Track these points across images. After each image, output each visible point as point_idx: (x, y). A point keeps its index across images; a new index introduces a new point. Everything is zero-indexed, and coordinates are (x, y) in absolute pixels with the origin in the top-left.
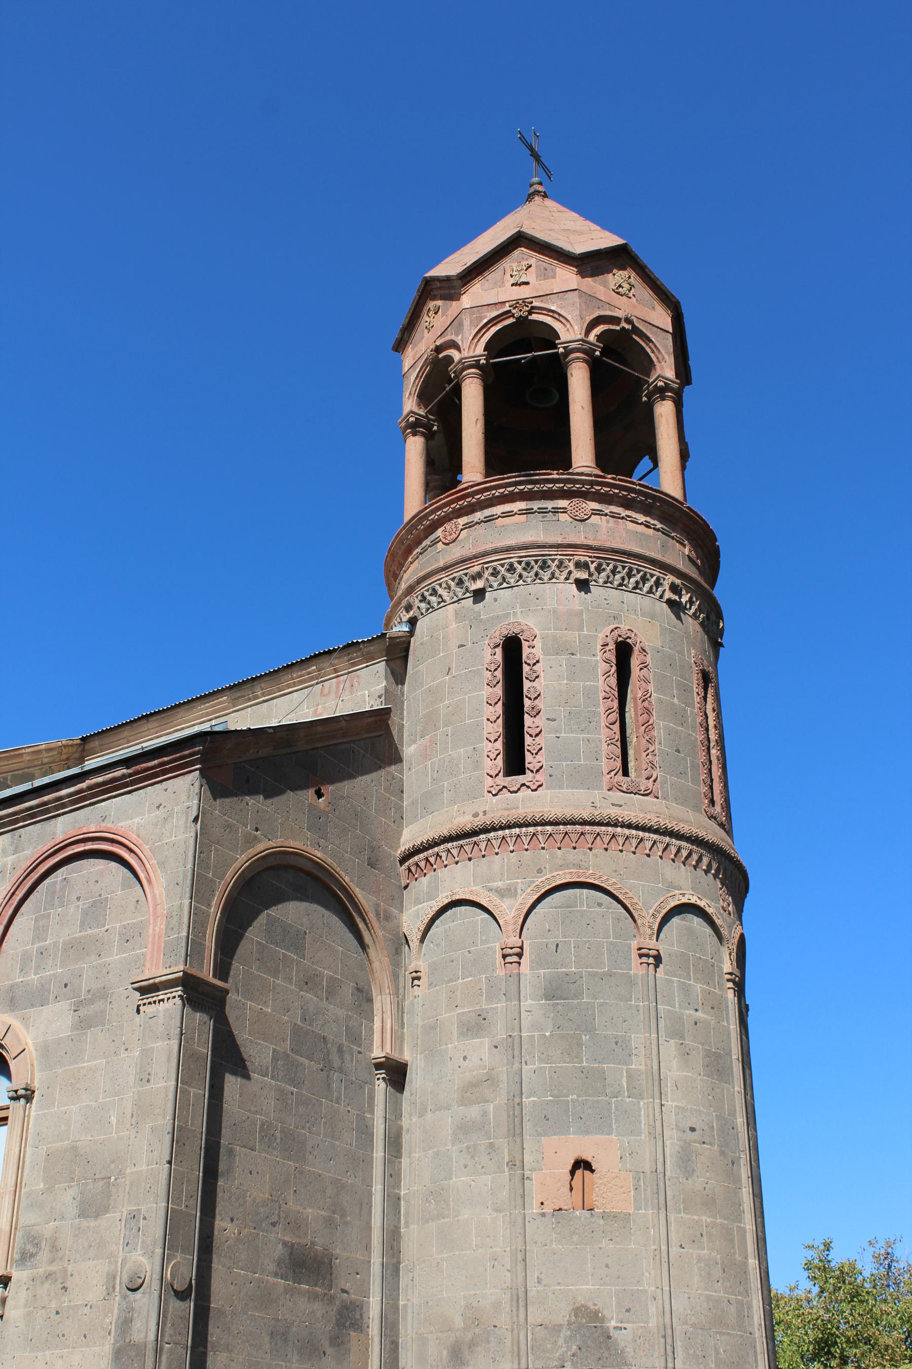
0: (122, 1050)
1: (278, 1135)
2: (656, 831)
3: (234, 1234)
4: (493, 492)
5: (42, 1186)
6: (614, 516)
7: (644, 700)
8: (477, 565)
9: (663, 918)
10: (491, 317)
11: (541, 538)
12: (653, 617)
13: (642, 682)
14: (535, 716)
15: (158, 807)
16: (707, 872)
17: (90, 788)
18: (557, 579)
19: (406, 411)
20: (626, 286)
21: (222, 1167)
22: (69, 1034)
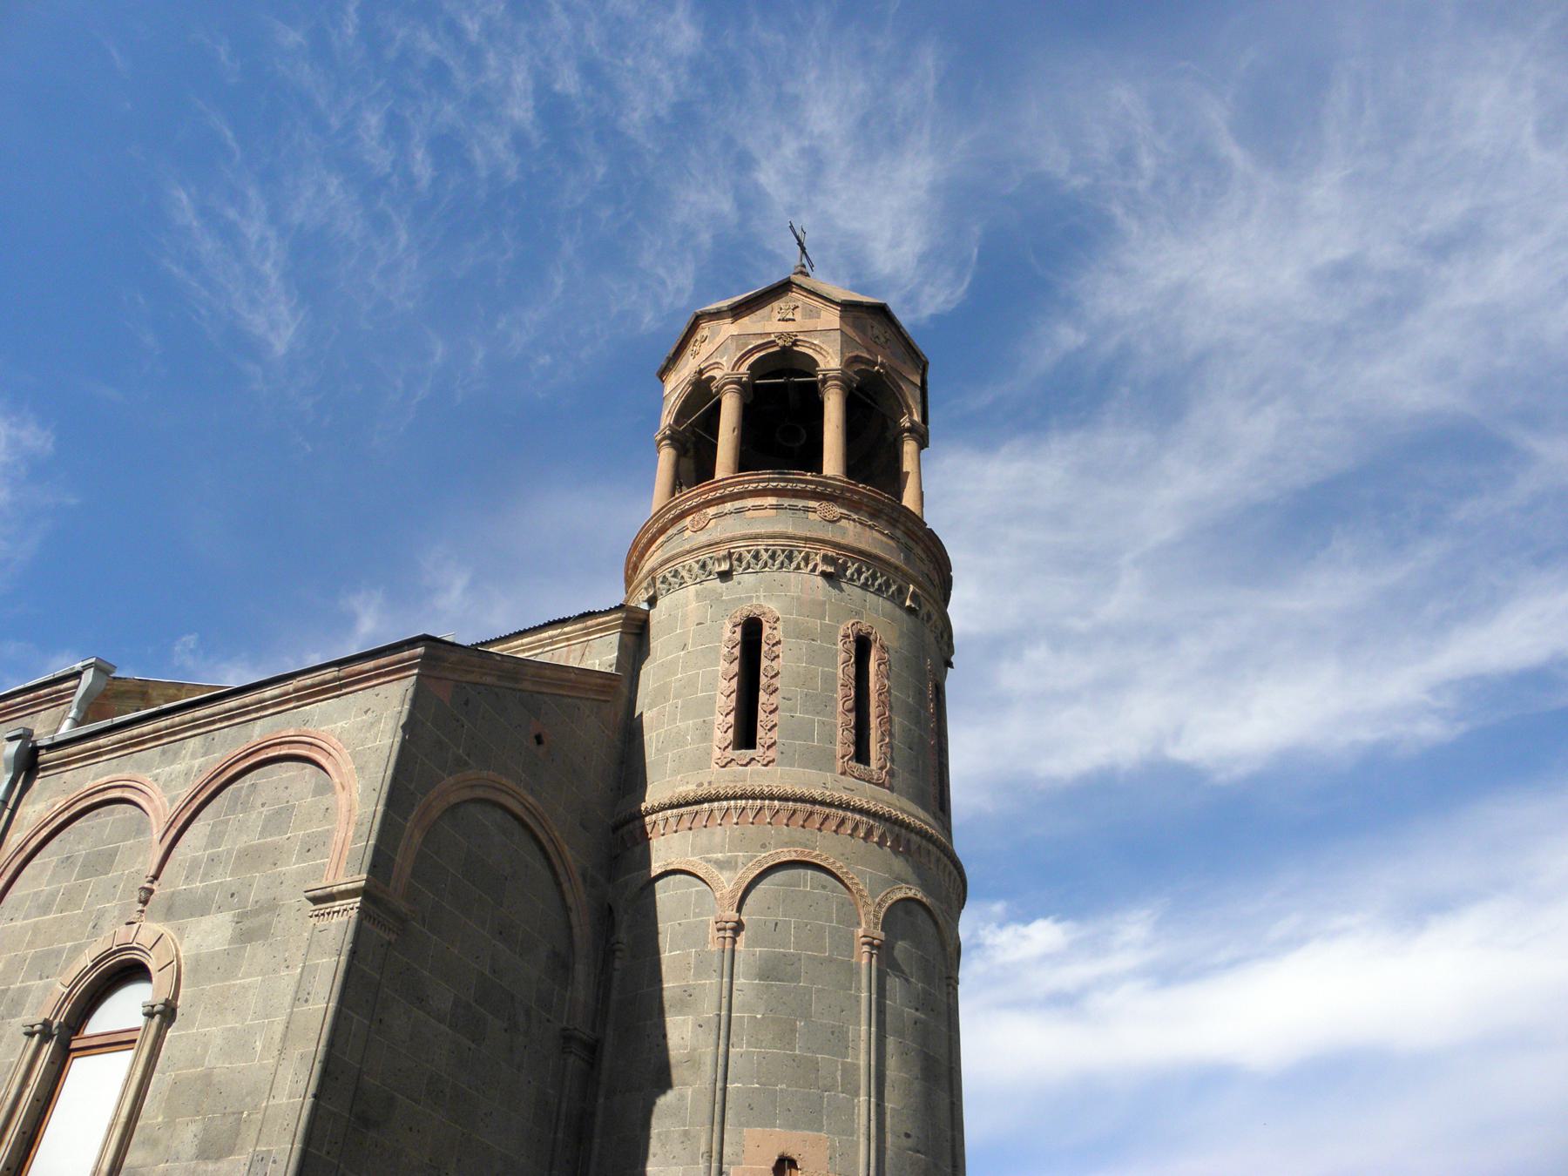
4: (746, 486)
11: (790, 531)
15: (366, 712)
20: (883, 339)
22: (226, 947)
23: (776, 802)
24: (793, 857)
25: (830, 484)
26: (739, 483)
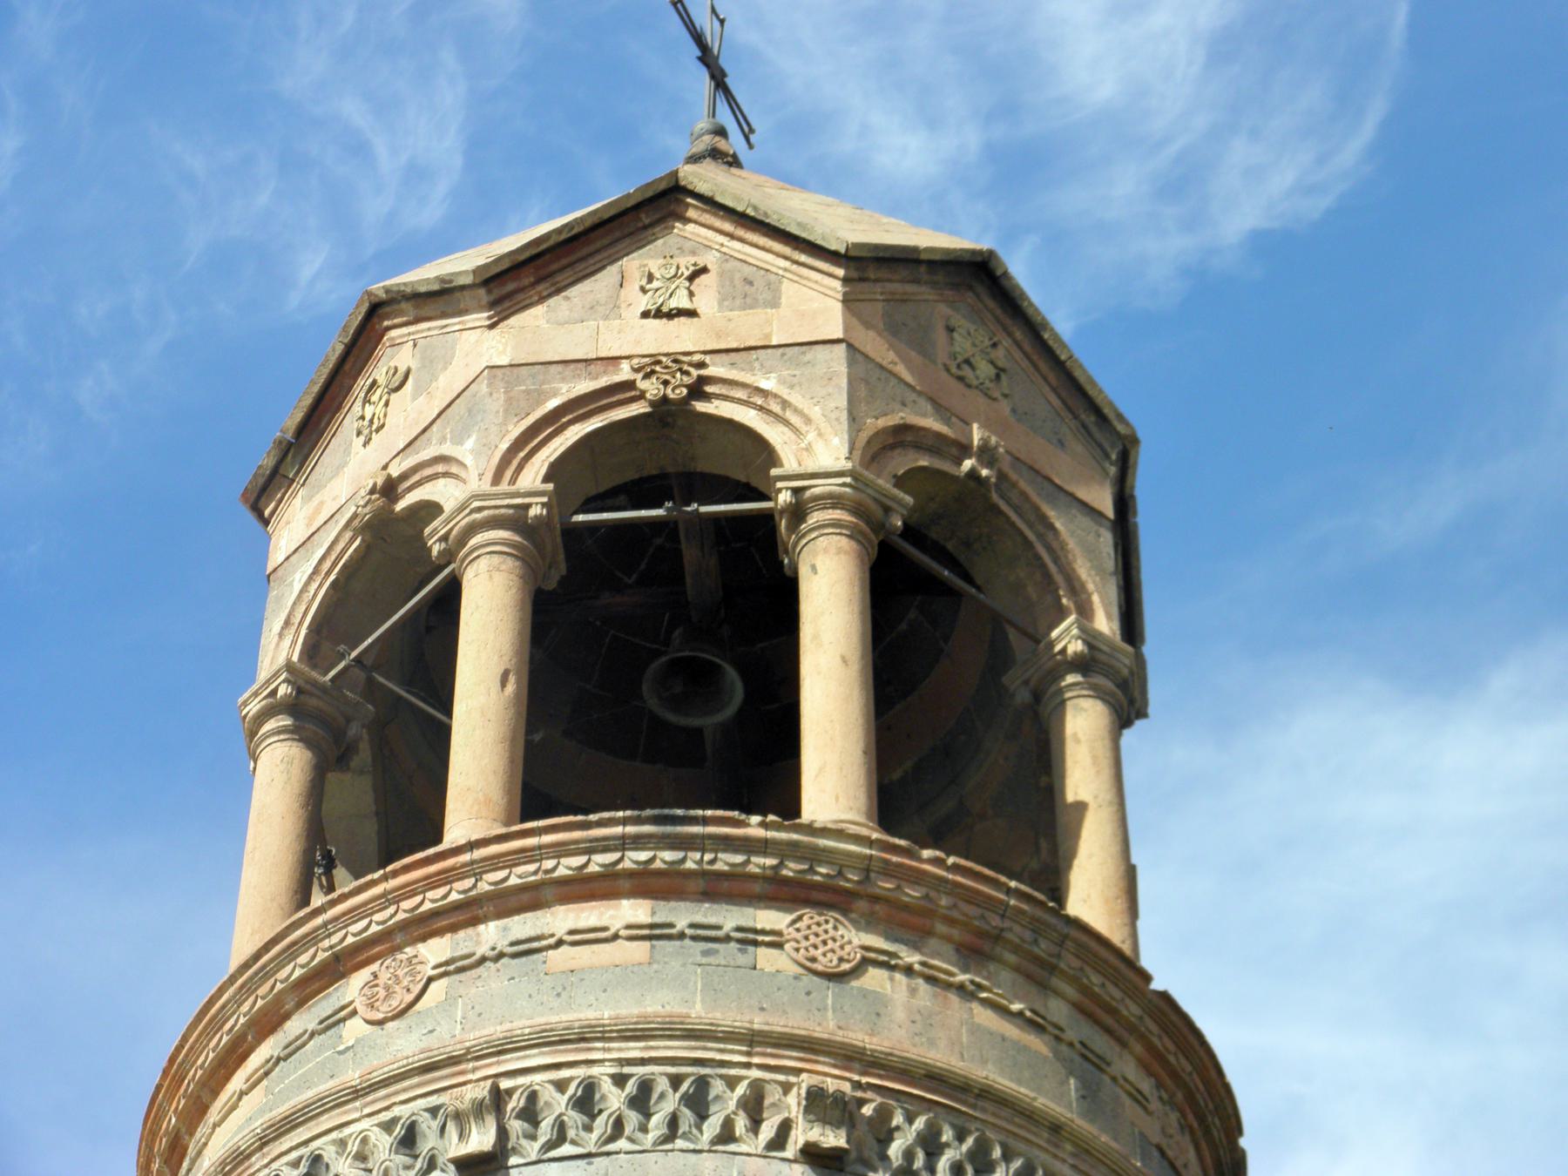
4: (549, 864)
8: (478, 1080)
10: (573, 395)
11: (698, 1011)
20: (985, 370)
25: (825, 850)
26: (525, 855)
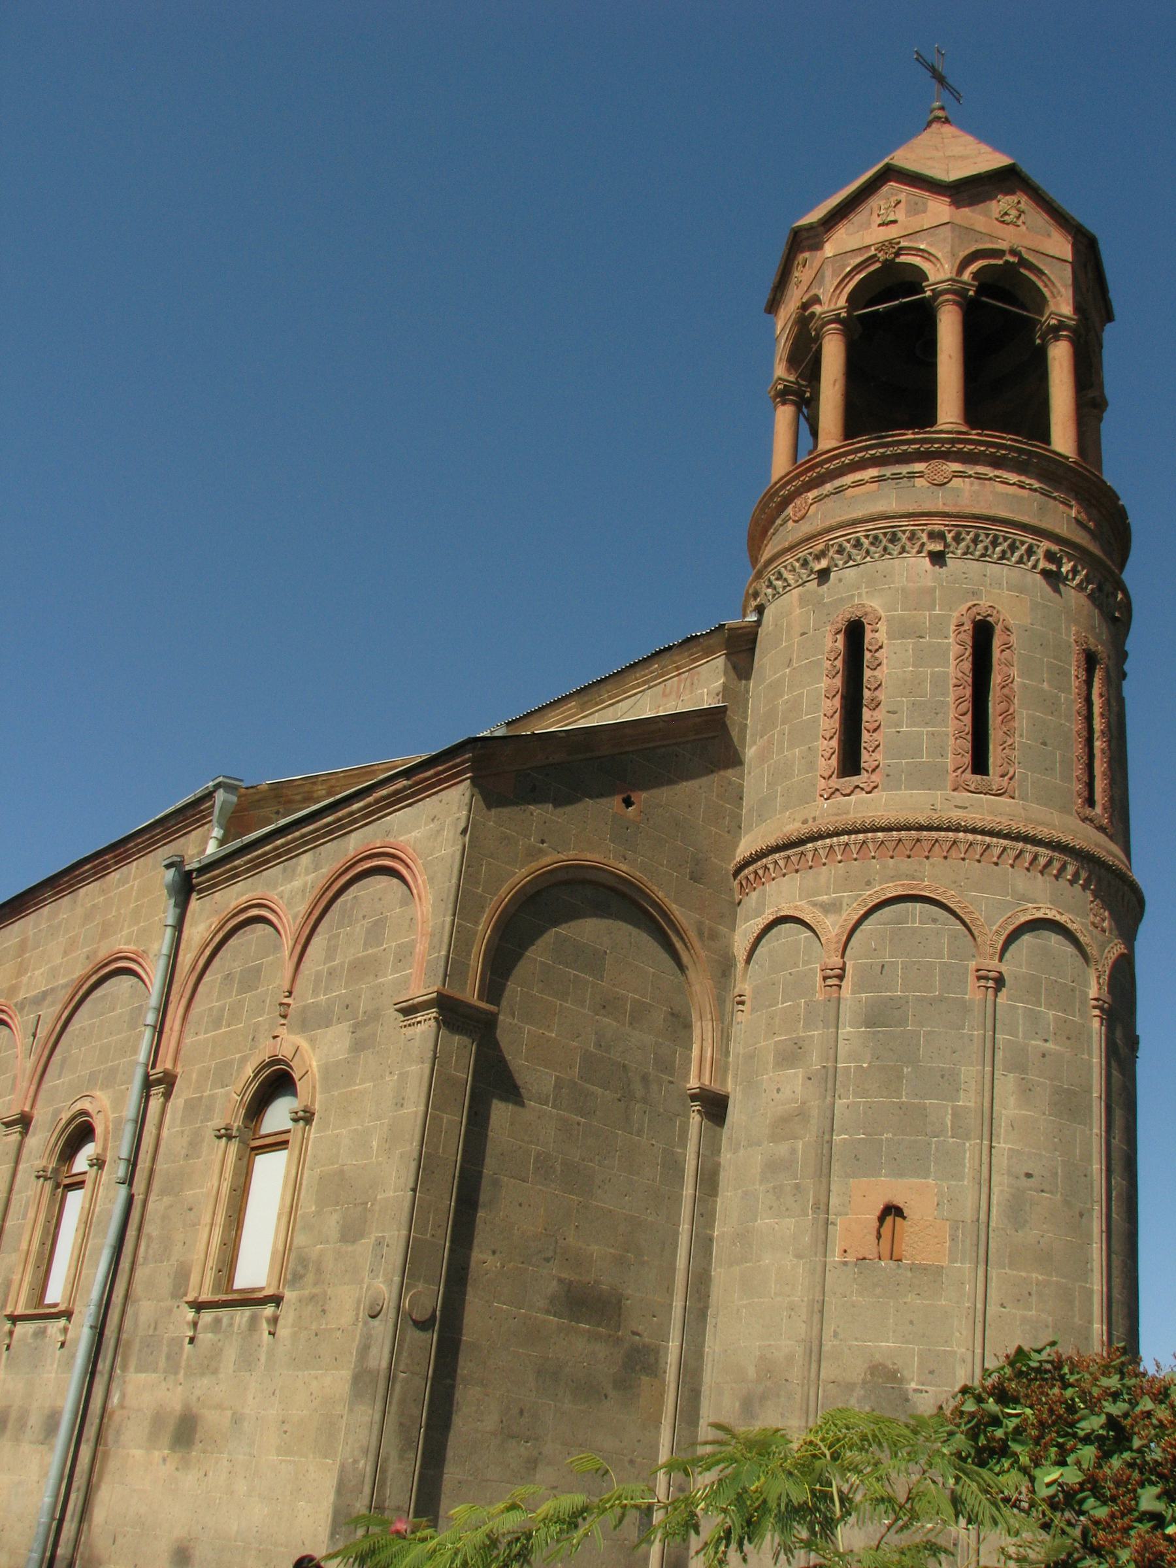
0: (387, 1073)
1: (558, 1167)
2: (1007, 836)
3: (496, 1267)
4: (843, 459)
5: (314, 1208)
6: (979, 477)
7: (1004, 687)
9: (1009, 936)
12: (1022, 590)
13: (1003, 666)
14: (874, 709)
15: (433, 820)
16: (1072, 882)
17: (377, 801)
18: (908, 553)
19: (775, 377)
20: (1014, 213)
21: (483, 1197)
23: (880, 834)
24: (900, 892)
